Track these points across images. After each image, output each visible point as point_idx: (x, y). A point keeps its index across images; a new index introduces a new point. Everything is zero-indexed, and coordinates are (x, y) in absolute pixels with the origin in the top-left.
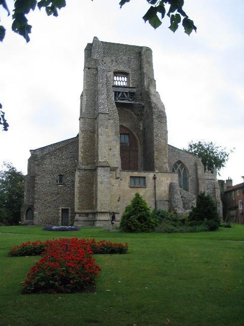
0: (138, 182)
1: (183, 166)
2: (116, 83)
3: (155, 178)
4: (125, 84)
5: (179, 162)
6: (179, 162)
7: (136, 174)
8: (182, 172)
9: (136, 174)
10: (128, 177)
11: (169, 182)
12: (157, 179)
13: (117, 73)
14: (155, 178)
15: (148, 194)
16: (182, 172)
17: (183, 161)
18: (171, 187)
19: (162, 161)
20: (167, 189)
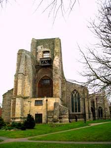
0: (38, 103)
1: (77, 92)
2: (44, 57)
3: (47, 100)
4: (48, 56)
5: (75, 90)
6: (75, 90)
7: (38, 99)
8: (77, 95)
9: (38, 99)
10: (34, 102)
11: (54, 102)
12: (48, 100)
13: (44, 52)
14: (47, 100)
15: (44, 108)
16: (77, 95)
17: (77, 89)
18: (55, 104)
19: (57, 91)
20: (53, 105)
